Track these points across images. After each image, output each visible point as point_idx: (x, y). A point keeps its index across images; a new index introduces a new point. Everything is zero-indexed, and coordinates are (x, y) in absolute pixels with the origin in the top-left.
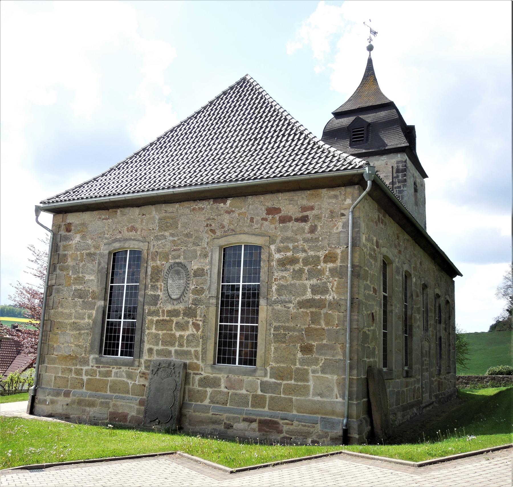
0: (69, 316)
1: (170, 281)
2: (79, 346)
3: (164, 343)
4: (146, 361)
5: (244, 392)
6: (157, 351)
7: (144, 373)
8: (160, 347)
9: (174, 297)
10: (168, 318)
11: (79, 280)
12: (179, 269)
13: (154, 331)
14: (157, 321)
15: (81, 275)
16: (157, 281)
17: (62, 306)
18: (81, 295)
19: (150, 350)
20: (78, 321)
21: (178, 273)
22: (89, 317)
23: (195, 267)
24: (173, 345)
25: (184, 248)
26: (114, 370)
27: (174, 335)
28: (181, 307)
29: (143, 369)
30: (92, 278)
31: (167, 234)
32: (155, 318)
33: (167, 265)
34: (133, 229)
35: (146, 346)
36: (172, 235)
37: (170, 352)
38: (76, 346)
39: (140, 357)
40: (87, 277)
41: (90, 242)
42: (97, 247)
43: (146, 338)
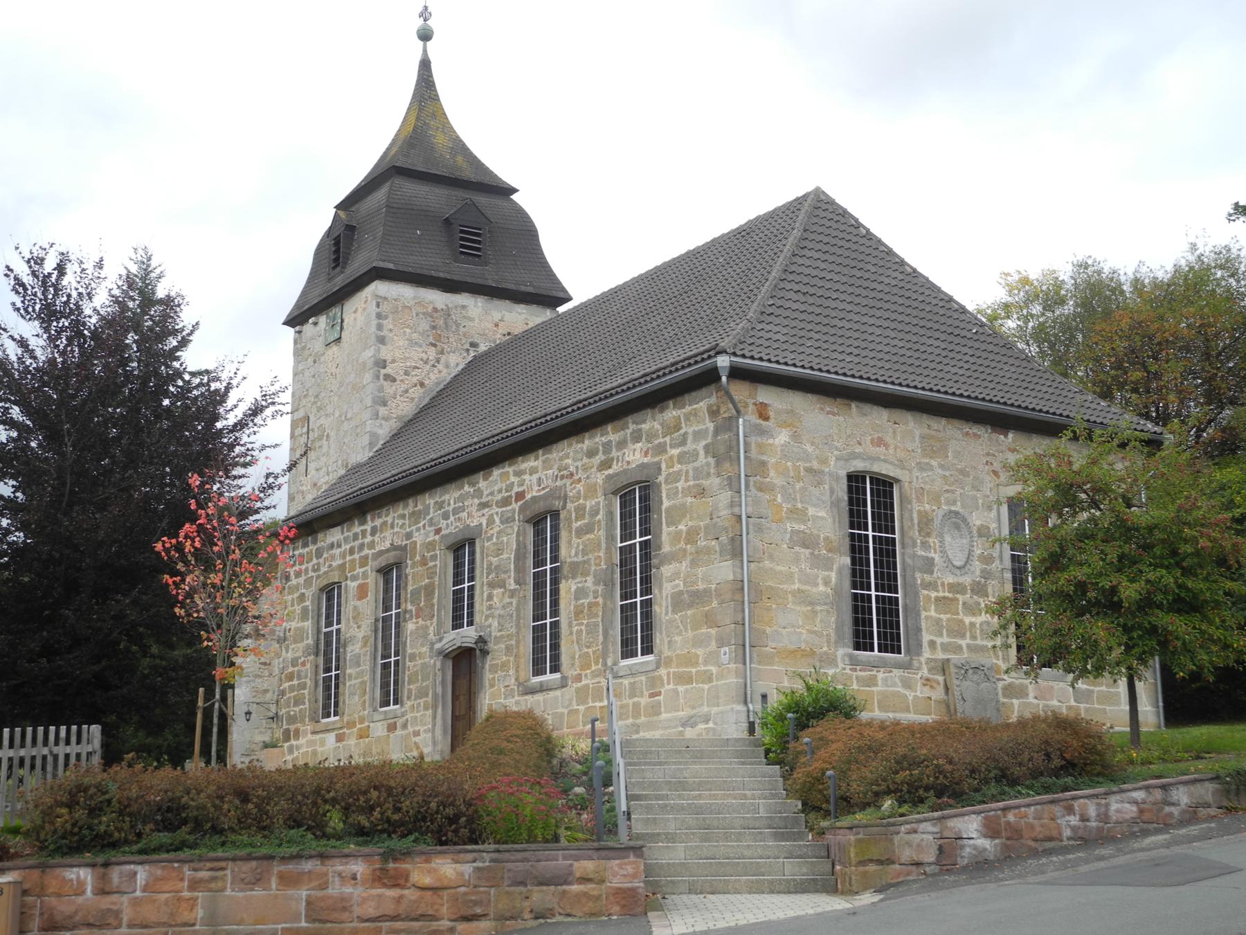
0: (789, 578)
1: (948, 538)
2: (815, 632)
3: (951, 633)
4: (929, 661)
5: (1055, 703)
6: (942, 644)
7: (928, 680)
8: (946, 639)
9: (958, 564)
10: (950, 595)
11: (798, 514)
12: (957, 521)
13: (933, 613)
14: (938, 599)
15: (799, 506)
16: (928, 535)
17: (771, 557)
18: (806, 541)
19: (932, 644)
20: (807, 588)
21: (958, 527)
22: (826, 583)
23: (978, 523)
24: (963, 636)
25: (959, 491)
26: (881, 676)
27: (962, 621)
28: (967, 580)
29: (925, 672)
30: (822, 514)
31: (934, 463)
32: (933, 595)
33: (941, 513)
34: (880, 442)
35: (926, 637)
36: (942, 466)
37: (960, 648)
38: (810, 632)
39: (919, 654)
40: (811, 511)
41: (809, 448)
42: (824, 461)
43: (923, 624)
